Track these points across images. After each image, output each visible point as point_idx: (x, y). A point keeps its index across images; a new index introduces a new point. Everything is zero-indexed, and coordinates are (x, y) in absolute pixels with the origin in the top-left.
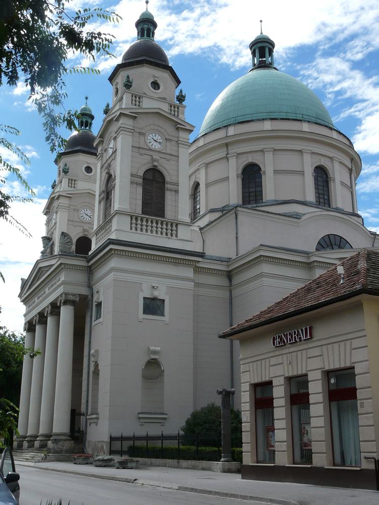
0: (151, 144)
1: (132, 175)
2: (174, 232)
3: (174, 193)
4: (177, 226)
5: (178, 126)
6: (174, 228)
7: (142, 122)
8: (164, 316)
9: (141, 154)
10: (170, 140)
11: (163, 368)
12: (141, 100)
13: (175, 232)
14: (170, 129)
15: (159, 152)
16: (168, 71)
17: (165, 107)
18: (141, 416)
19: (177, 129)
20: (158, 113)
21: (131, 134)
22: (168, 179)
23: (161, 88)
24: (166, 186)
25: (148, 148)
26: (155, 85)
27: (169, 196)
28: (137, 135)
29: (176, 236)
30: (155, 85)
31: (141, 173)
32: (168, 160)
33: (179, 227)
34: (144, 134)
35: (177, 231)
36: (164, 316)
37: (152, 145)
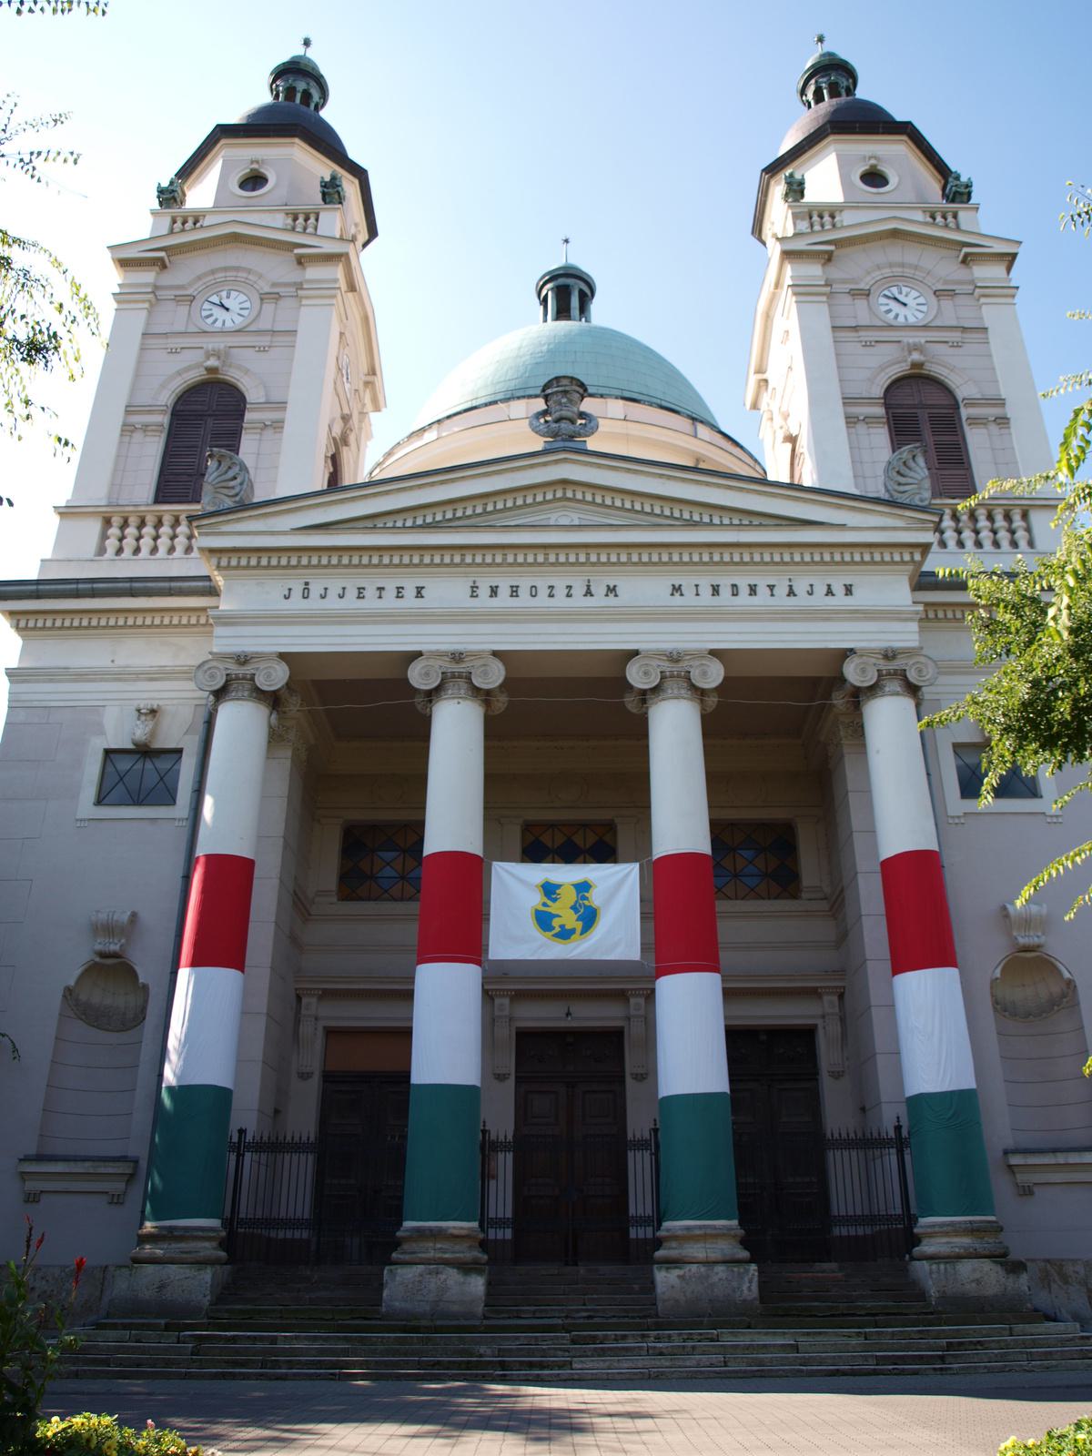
0: (891, 315)
1: (848, 401)
2: (1021, 535)
3: (993, 428)
4: (1025, 516)
5: (965, 250)
6: (1018, 522)
7: (856, 267)
8: (1041, 797)
9: (867, 345)
10: (952, 294)
11: (1067, 975)
12: (836, 220)
13: (1026, 534)
14: (945, 268)
15: (925, 327)
16: (905, 138)
17: (915, 220)
18: (1015, 1160)
19: (965, 261)
20: (895, 234)
21: (824, 299)
22: (962, 392)
23: (893, 180)
24: (965, 412)
25: (880, 324)
26: (874, 178)
27: (977, 442)
28: (848, 299)
29: (1031, 544)
30: (874, 178)
31: (878, 391)
32: (957, 345)
33: (1035, 517)
34: (867, 294)
35: (1028, 530)
36: (1041, 797)
37: (897, 316)
